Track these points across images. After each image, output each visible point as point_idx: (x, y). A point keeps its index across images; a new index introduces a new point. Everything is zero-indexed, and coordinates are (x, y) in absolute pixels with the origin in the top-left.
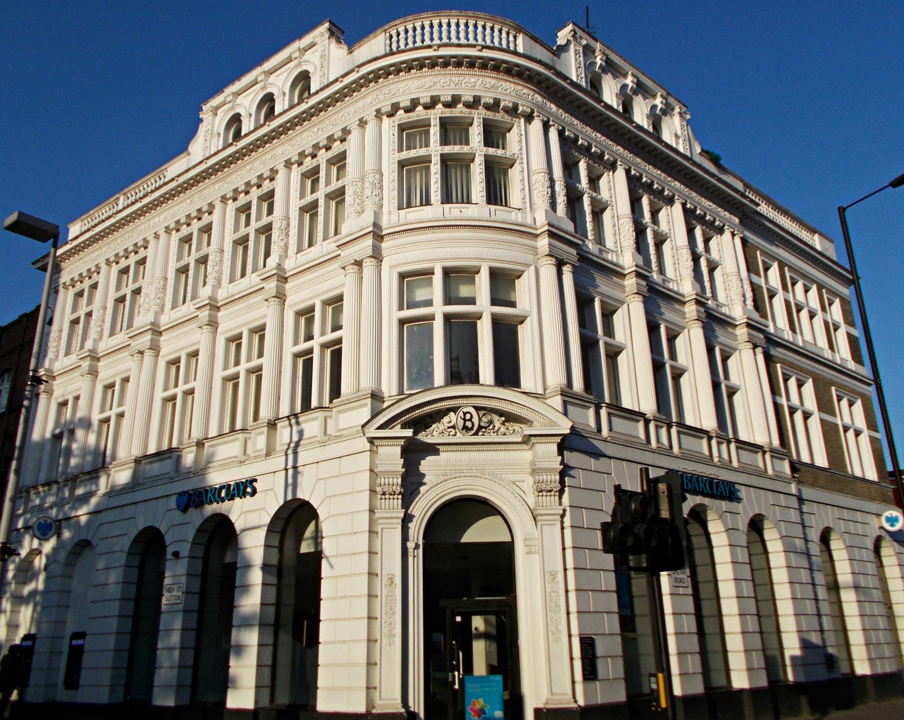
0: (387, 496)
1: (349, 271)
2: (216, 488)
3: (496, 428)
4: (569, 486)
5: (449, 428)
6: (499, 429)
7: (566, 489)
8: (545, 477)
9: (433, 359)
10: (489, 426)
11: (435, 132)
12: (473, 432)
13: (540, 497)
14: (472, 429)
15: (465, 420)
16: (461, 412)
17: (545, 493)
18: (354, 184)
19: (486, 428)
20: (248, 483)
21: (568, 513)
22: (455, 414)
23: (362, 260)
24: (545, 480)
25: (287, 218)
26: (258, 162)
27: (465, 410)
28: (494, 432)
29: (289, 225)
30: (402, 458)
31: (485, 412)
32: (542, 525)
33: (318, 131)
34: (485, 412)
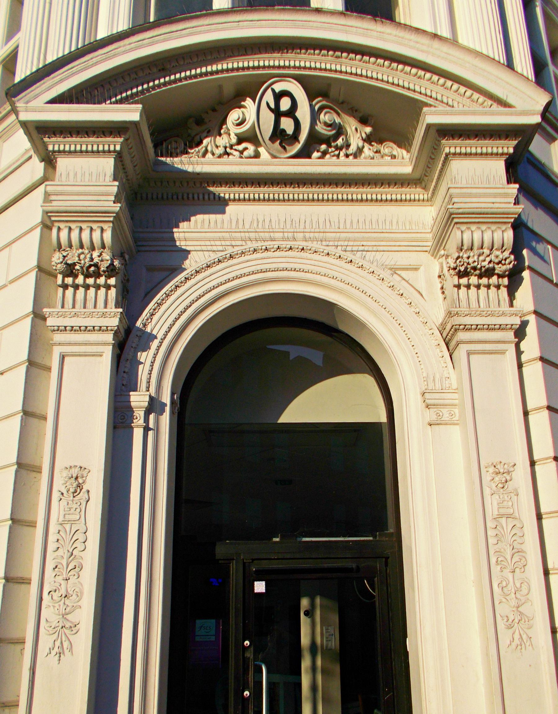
0: (80, 280)
3: (353, 149)
4: (530, 268)
6: (360, 151)
7: (526, 274)
8: (477, 236)
10: (336, 137)
12: (297, 147)
13: (463, 290)
14: (295, 137)
15: (278, 113)
16: (269, 91)
17: (474, 280)
19: (328, 141)
21: (532, 330)
22: (254, 102)
24: (476, 244)
27: (279, 87)
28: (347, 156)
30: (115, 179)
31: (324, 103)
32: (469, 354)
34: (324, 103)
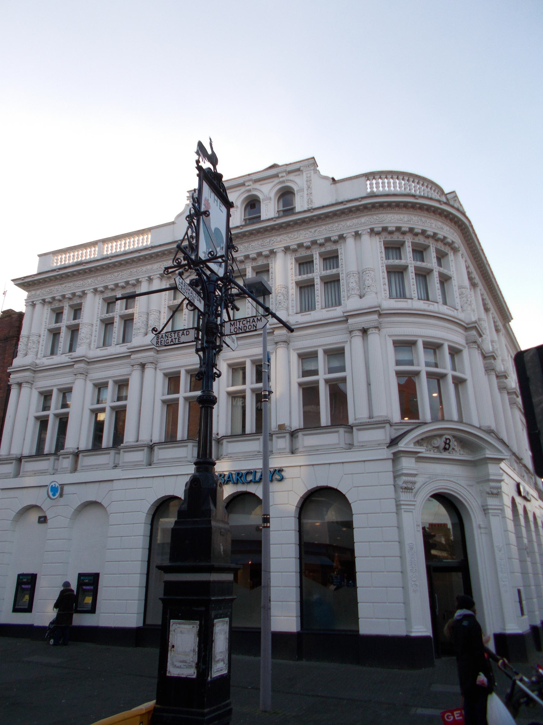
1: (356, 334)
2: (242, 474)
5: (434, 447)
9: (417, 401)
11: (408, 250)
14: (448, 449)
15: (446, 443)
18: (355, 275)
20: (277, 471)
23: (368, 329)
25: (286, 288)
26: (256, 242)
27: (448, 437)
29: (288, 292)
33: (315, 231)
